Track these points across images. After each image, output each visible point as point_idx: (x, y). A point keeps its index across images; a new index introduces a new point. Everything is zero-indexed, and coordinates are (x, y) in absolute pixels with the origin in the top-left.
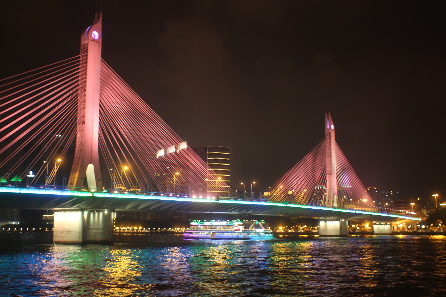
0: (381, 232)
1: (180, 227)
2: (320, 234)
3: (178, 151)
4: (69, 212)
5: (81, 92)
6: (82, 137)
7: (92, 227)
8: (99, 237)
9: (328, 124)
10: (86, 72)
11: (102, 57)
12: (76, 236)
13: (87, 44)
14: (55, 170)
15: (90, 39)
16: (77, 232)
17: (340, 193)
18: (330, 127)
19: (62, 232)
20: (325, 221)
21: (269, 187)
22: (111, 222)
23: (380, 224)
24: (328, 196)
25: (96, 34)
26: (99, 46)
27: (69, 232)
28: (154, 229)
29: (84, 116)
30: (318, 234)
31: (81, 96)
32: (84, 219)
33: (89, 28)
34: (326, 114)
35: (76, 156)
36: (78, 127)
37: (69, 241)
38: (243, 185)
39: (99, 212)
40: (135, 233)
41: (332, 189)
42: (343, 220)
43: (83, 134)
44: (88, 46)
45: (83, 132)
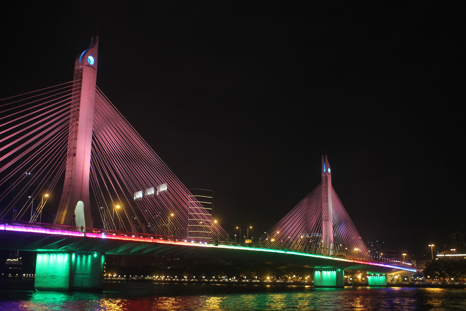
0: (376, 284)
1: (159, 275)
2: (314, 285)
3: (158, 193)
4: (55, 255)
5: (73, 121)
6: (72, 171)
7: (78, 272)
8: (86, 284)
9: (325, 167)
10: (80, 99)
11: (96, 85)
12: (61, 282)
13: (82, 70)
14: (42, 205)
15: (85, 64)
16: (63, 277)
17: (336, 241)
18: (327, 170)
19: (45, 277)
20: (321, 270)
21: (265, 233)
22: (101, 266)
23: (375, 275)
24: (324, 244)
25: (91, 60)
26: (95, 73)
27: (53, 277)
28: (130, 276)
29: (75, 148)
30: (313, 285)
31: (73, 126)
32: (72, 263)
33: (84, 52)
34: (323, 157)
35: (64, 191)
36: (68, 160)
37: (53, 287)
38: (239, 229)
39: (87, 255)
40: (109, 280)
41: (328, 236)
43: (74, 168)
44: (82, 71)
45: (73, 165)
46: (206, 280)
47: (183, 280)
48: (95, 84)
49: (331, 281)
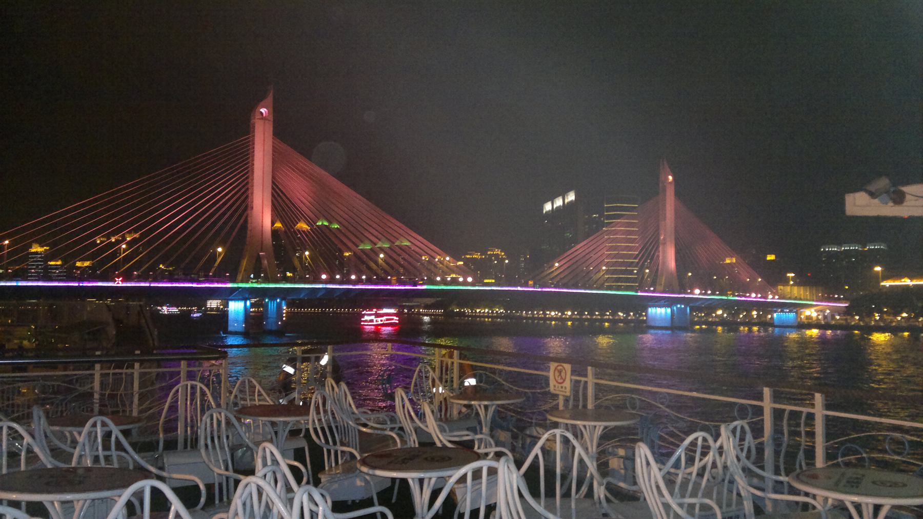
0: (783, 323)
7: (269, 316)
11: (273, 135)
29: (253, 202)
36: (249, 212)
42: (683, 306)
46: (589, 317)
47: (584, 317)
48: (272, 134)
49: (662, 319)
